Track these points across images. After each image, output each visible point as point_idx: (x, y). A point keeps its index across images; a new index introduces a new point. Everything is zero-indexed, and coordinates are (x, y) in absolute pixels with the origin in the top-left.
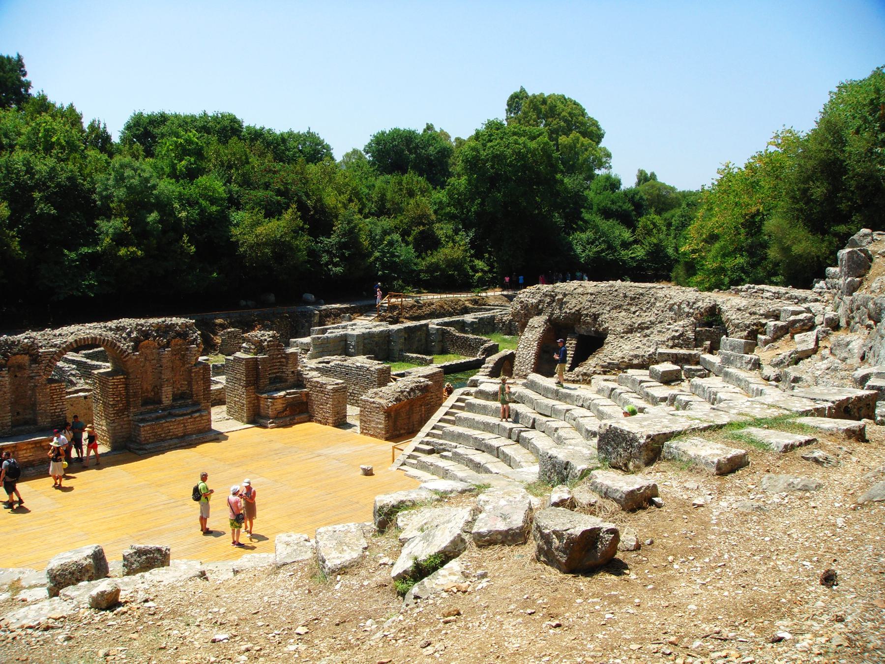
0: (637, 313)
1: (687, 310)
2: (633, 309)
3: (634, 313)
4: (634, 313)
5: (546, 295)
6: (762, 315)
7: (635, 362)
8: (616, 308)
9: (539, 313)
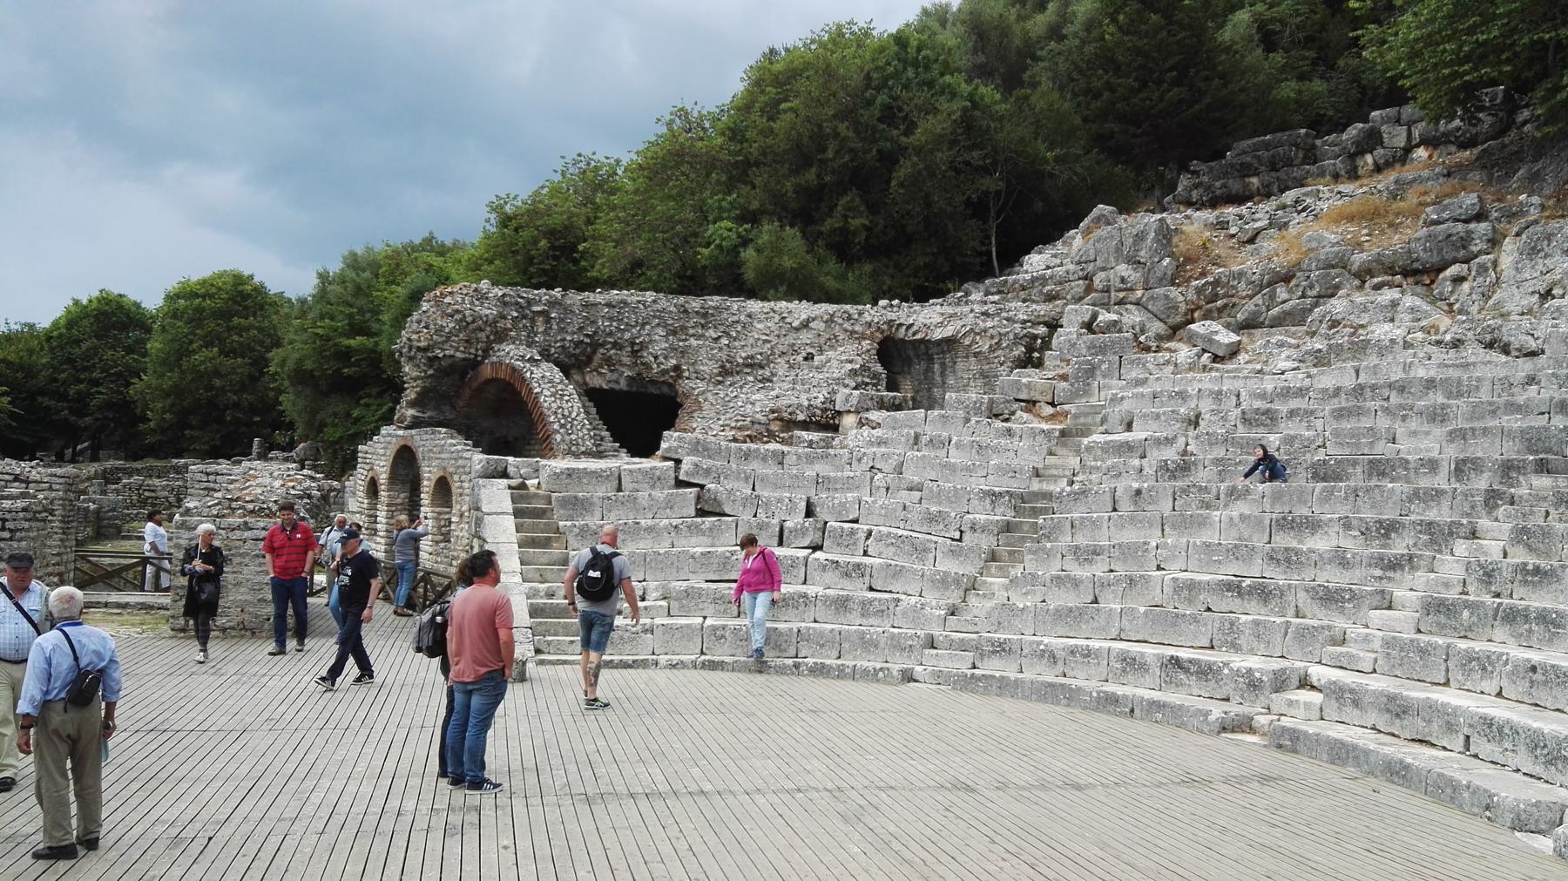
0: (725, 341)
1: (847, 325)
2: (712, 333)
3: (717, 339)
4: (717, 339)
5: (505, 304)
6: (1024, 322)
7: (801, 417)
8: (674, 333)
9: (501, 336)
